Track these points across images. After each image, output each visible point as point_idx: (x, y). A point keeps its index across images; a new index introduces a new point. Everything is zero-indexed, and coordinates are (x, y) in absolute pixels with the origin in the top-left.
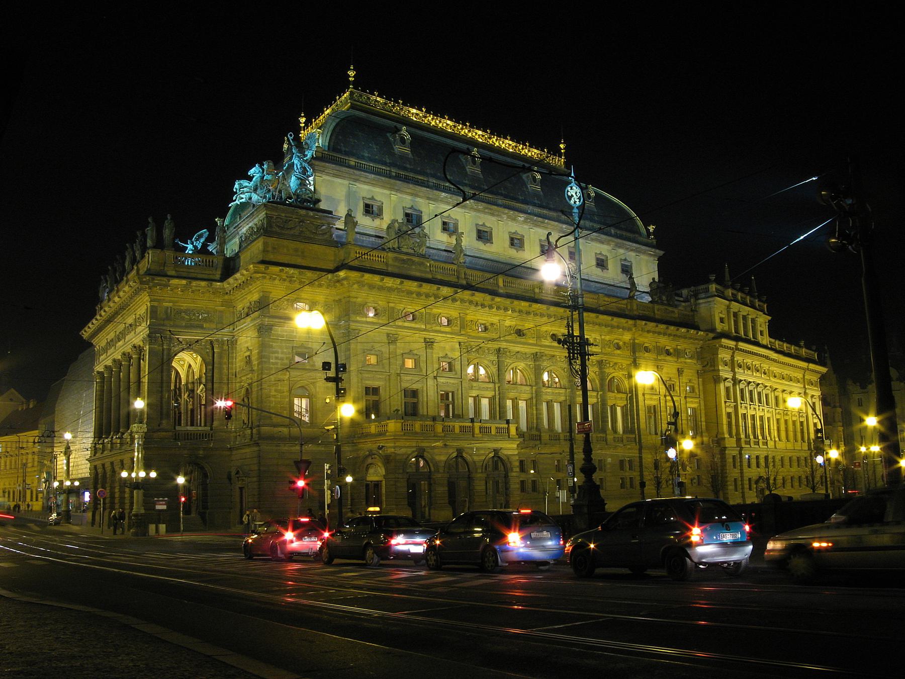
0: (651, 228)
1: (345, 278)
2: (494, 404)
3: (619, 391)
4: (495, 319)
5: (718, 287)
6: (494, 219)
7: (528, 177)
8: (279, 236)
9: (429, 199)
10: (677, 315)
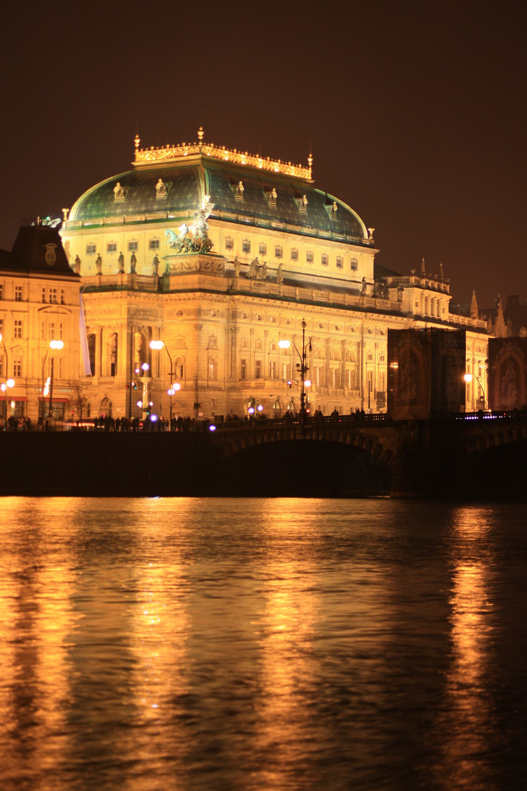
0: (371, 230)
1: (238, 300)
2: (290, 368)
3: (351, 361)
4: (293, 316)
5: (417, 278)
6: (283, 240)
7: (299, 202)
8: (205, 273)
9: (255, 233)
10: (389, 305)
